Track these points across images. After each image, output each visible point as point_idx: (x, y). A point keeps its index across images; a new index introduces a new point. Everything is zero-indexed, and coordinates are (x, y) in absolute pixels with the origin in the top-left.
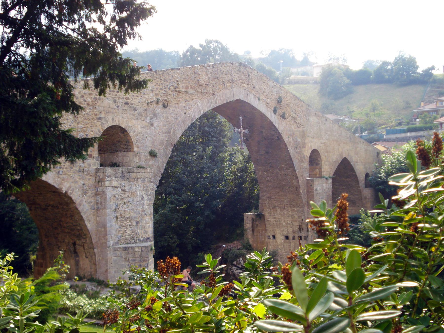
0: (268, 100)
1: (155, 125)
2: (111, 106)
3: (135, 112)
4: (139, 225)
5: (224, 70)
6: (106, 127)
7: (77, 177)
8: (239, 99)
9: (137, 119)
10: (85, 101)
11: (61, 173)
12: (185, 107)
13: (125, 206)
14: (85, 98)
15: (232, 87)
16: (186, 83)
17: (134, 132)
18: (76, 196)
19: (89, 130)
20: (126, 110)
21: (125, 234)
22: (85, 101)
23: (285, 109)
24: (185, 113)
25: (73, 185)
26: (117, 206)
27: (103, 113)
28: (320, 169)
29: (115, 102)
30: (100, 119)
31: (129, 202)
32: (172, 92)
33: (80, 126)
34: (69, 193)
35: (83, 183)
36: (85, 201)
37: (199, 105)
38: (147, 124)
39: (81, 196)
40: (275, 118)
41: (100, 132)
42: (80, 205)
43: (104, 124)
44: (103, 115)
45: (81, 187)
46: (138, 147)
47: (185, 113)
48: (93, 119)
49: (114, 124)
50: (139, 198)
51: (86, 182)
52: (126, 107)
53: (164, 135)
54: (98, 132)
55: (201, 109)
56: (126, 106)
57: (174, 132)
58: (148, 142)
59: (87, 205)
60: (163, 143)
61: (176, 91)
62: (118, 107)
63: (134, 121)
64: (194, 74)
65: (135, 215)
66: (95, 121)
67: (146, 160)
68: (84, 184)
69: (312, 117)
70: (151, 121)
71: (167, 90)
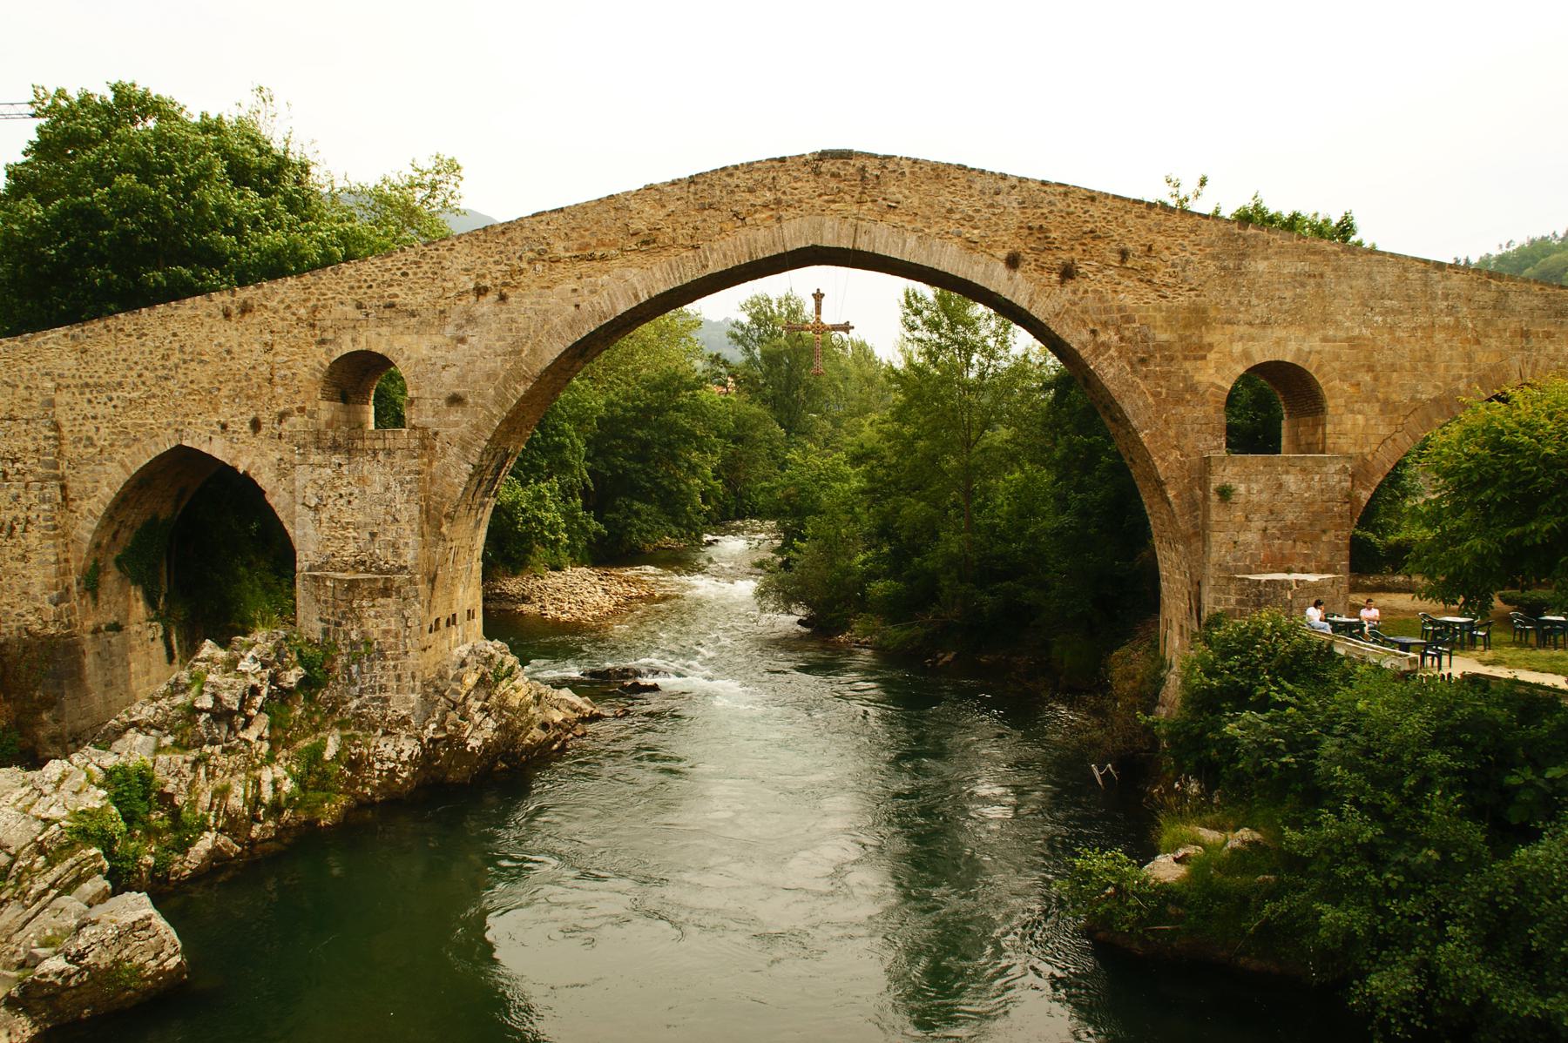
0: (976, 232)
1: (470, 340)
2: (350, 316)
3: (414, 320)
4: (377, 539)
5: (738, 182)
6: (337, 355)
7: (265, 448)
9: (417, 333)
10: (294, 314)
12: (575, 290)
13: (342, 501)
14: (294, 310)
15: (779, 219)
16: (583, 236)
17: (409, 359)
18: (265, 480)
19: (300, 363)
20: (388, 319)
21: (342, 553)
22: (294, 314)
23: (1080, 248)
24: (577, 306)
25: (258, 460)
26: (321, 499)
27: (331, 330)
28: (1324, 425)
29: (359, 306)
30: (322, 342)
31: (351, 494)
32: (529, 263)
33: (279, 359)
34: (252, 473)
37: (635, 280)
38: (447, 341)
40: (1010, 279)
41: (322, 365)
43: (331, 350)
44: (329, 335)
45: (273, 465)
46: (417, 389)
47: (577, 306)
48: (310, 344)
50: (379, 489)
51: (286, 457)
52: (387, 313)
53: (499, 359)
54: (318, 366)
55: (639, 287)
56: (387, 312)
57: (533, 351)
58: (449, 377)
59: (287, 496)
60: (496, 376)
62: (367, 315)
63: (408, 339)
64: (613, 213)
65: (369, 520)
66: (314, 347)
67: (436, 413)
69: (1267, 258)
70: (460, 333)
71: (515, 261)
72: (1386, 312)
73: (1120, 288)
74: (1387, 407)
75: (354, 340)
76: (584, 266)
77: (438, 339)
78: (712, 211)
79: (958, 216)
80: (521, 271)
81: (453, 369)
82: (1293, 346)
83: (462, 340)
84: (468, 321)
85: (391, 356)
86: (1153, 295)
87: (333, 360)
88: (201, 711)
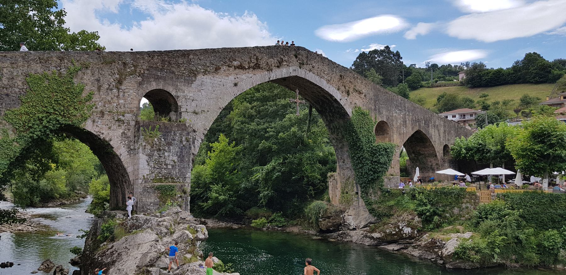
8: (296, 76)
11: (99, 123)
28: (390, 138)
34: (107, 139)
35: (122, 132)
36: (124, 147)
39: (120, 142)
42: (119, 148)
49: (158, 88)
51: (125, 131)
61: (226, 66)
62: (163, 74)
68: (124, 133)
72: (399, 110)
73: (356, 98)
74: (400, 134)
75: (157, 85)
76: (237, 71)
77: (190, 89)
78: (272, 59)
79: (326, 73)
80: (220, 69)
81: (196, 102)
82: (385, 117)
83: (199, 91)
84: (201, 84)
85: (173, 93)
86: (362, 101)
87: (148, 91)
88: (200, 240)
